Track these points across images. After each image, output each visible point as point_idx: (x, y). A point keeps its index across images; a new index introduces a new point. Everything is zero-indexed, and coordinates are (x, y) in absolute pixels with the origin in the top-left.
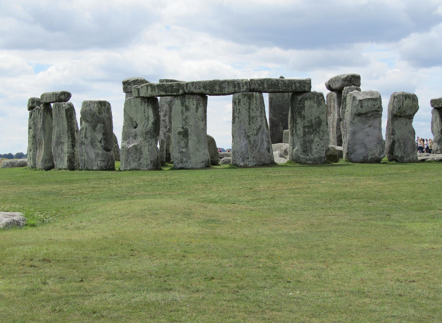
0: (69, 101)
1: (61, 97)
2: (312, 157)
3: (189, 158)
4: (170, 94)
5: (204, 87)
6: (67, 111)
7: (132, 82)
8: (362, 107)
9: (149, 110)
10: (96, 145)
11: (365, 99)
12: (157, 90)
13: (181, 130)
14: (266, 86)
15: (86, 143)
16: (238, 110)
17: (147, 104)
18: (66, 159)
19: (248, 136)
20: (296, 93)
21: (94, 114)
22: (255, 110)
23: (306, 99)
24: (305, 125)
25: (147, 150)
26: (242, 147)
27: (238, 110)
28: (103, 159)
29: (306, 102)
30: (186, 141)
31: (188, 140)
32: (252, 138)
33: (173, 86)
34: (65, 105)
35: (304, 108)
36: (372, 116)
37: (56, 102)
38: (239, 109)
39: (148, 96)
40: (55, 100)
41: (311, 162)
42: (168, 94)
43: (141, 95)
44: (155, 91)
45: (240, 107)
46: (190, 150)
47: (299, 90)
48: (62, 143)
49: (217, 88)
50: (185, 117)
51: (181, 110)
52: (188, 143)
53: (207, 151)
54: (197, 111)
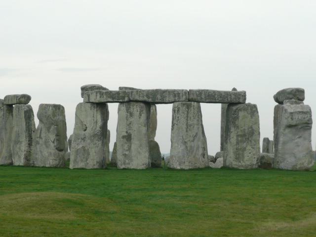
0: (29, 104)
1: (21, 99)
2: (244, 164)
3: (131, 160)
4: (116, 100)
5: (147, 96)
6: (26, 112)
7: (90, 88)
8: (292, 119)
9: (98, 114)
10: (50, 145)
11: (296, 112)
12: (105, 96)
13: (125, 134)
14: (203, 96)
16: (177, 118)
17: (96, 109)
18: (23, 157)
19: (185, 142)
20: (231, 104)
21: (48, 116)
22: (192, 118)
23: (240, 110)
24: (239, 134)
25: (94, 151)
26: (179, 152)
27: (177, 118)
28: (55, 158)
29: (240, 113)
31: (131, 144)
32: (189, 144)
34: (24, 108)
35: (238, 118)
36: (302, 128)
37: (17, 104)
38: (178, 117)
39: (97, 102)
40: (16, 103)
41: (242, 168)
42: (115, 100)
43: (91, 101)
45: (179, 115)
47: (234, 101)
48: (21, 143)
49: (159, 97)
50: (129, 122)
51: (126, 116)
52: (130, 147)
53: (147, 154)
54: (140, 118)
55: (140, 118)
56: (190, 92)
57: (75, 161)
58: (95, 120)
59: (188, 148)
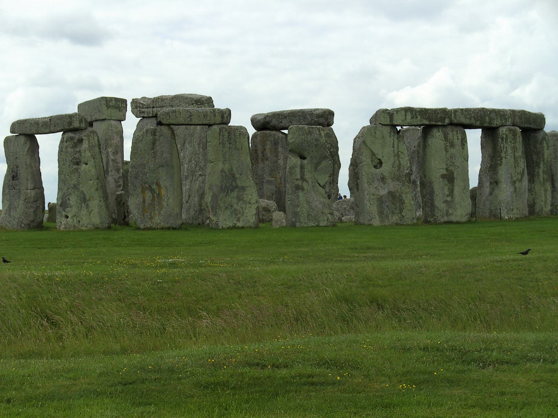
7: (206, 100)
9: (402, 143)
12: (419, 117)
13: (445, 172)
15: (305, 188)
16: (505, 149)
25: (411, 198)
30: (451, 187)
31: (453, 186)
32: (517, 185)
33: (438, 113)
44: (417, 117)
46: (456, 199)
48: (243, 189)
49: (487, 119)
51: (444, 146)
54: (463, 148)
55: (463, 148)
56: (513, 112)
57: (381, 213)
58: (396, 151)
59: (518, 190)
